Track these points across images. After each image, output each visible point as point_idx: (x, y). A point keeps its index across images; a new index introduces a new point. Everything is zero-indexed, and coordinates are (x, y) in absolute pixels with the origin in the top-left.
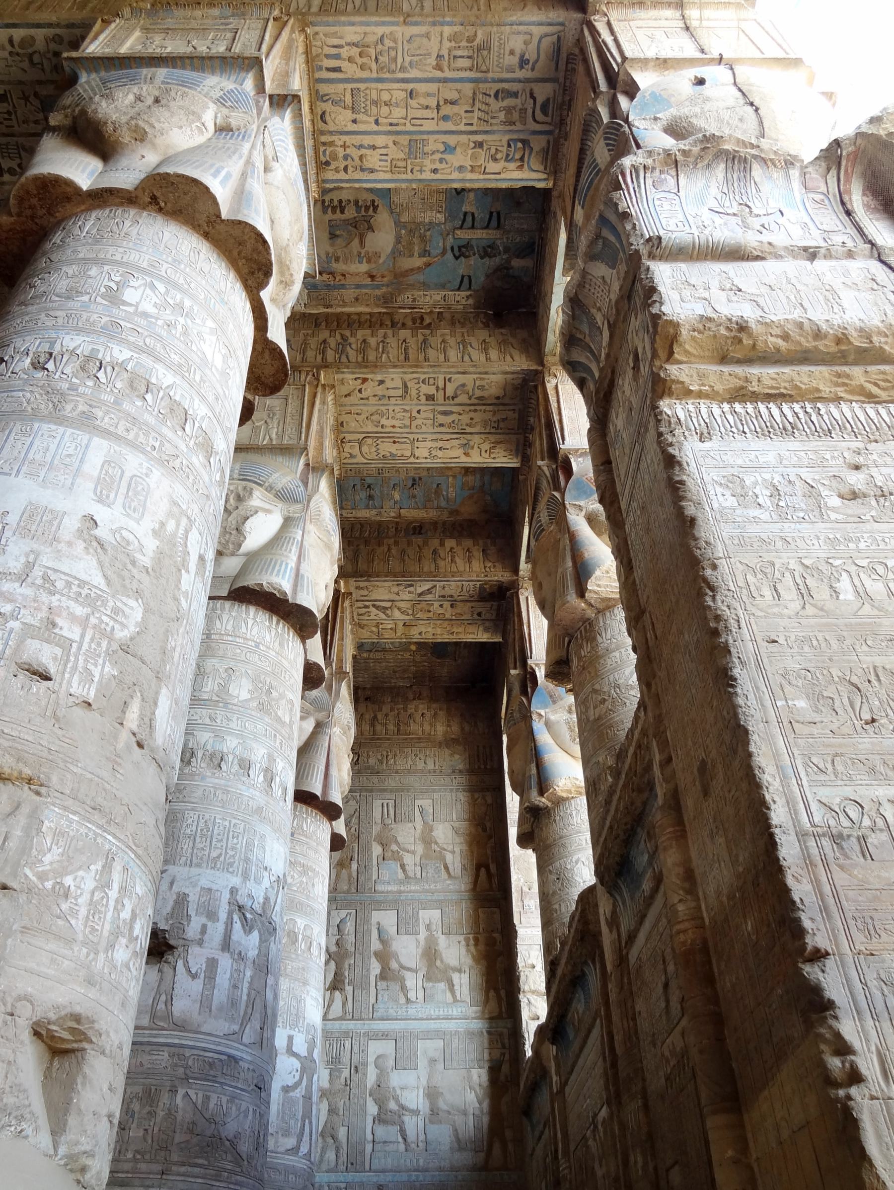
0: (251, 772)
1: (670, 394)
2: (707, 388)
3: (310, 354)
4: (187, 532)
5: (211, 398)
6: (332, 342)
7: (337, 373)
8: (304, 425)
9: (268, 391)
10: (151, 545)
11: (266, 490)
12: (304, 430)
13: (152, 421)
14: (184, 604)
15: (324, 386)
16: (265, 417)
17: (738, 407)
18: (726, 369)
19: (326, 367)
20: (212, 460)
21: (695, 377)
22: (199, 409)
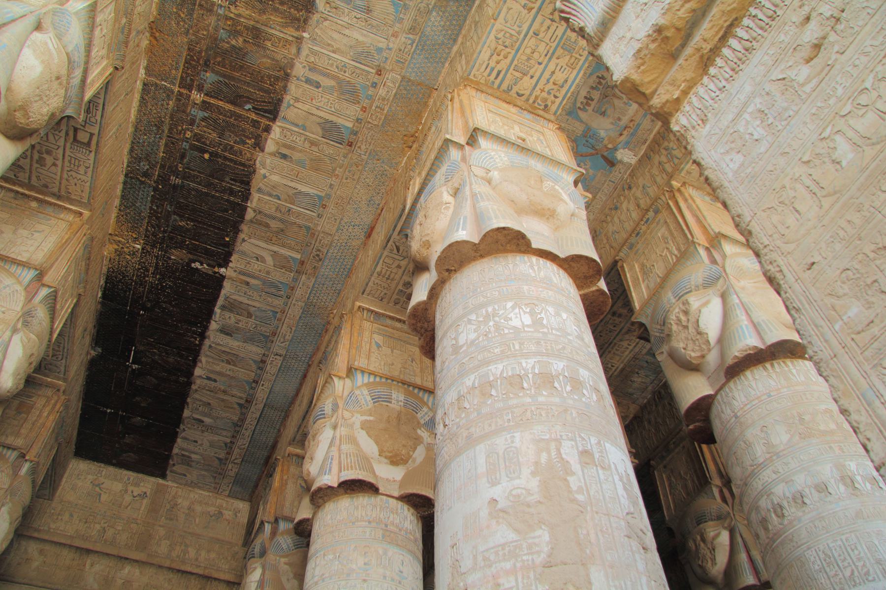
0: (830, 490)
1: (671, 115)
2: (683, 85)
3: (658, 179)
4: (558, 450)
5: (533, 348)
6: (663, 159)
7: (680, 172)
8: (684, 227)
9: (598, 277)
10: (534, 484)
11: (696, 290)
12: (687, 232)
13: (500, 405)
14: (580, 497)
15: (679, 190)
16: (664, 245)
17: (712, 71)
18: (681, 61)
19: (671, 177)
20: (556, 385)
21: (670, 88)
22: (528, 364)
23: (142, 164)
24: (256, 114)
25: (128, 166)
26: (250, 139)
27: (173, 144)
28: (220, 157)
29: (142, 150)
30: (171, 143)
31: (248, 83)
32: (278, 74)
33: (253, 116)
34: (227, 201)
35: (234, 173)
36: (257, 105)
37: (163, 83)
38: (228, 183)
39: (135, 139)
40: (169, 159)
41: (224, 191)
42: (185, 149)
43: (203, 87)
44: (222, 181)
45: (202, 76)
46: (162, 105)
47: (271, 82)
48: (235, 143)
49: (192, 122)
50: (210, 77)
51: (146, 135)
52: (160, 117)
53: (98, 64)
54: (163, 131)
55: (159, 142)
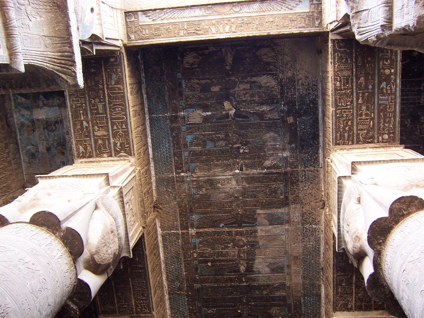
23: (175, 283)
24: (228, 227)
25: (168, 288)
26: (230, 243)
27: (189, 264)
28: (217, 261)
29: (173, 275)
30: (187, 264)
31: (216, 212)
32: (231, 199)
33: (227, 229)
34: (231, 286)
35: (229, 268)
36: (226, 222)
37: (172, 231)
38: (227, 275)
39: (167, 270)
40: (189, 274)
41: (226, 281)
42: (196, 265)
43: (194, 224)
44: (223, 275)
45: (191, 219)
46: (176, 244)
47: (228, 205)
48: (222, 249)
49: (195, 247)
50: (195, 217)
51: (172, 265)
52: (177, 252)
53: (133, 225)
54: (181, 259)
55: (181, 266)
